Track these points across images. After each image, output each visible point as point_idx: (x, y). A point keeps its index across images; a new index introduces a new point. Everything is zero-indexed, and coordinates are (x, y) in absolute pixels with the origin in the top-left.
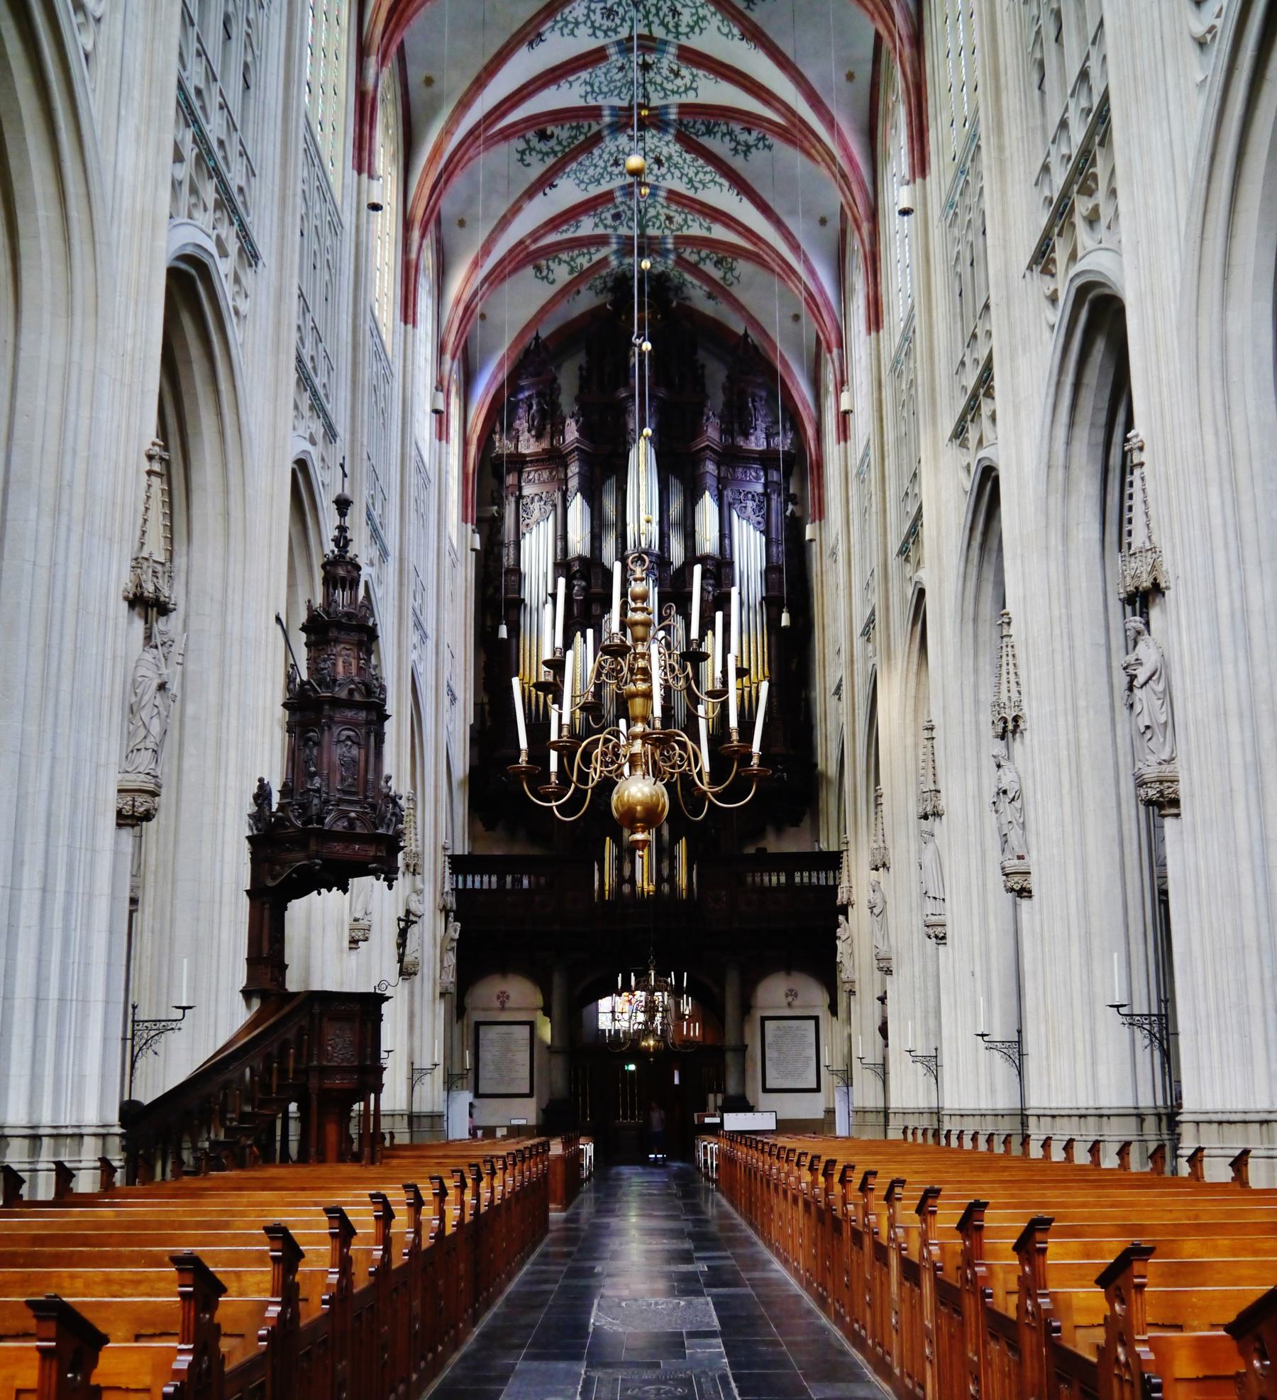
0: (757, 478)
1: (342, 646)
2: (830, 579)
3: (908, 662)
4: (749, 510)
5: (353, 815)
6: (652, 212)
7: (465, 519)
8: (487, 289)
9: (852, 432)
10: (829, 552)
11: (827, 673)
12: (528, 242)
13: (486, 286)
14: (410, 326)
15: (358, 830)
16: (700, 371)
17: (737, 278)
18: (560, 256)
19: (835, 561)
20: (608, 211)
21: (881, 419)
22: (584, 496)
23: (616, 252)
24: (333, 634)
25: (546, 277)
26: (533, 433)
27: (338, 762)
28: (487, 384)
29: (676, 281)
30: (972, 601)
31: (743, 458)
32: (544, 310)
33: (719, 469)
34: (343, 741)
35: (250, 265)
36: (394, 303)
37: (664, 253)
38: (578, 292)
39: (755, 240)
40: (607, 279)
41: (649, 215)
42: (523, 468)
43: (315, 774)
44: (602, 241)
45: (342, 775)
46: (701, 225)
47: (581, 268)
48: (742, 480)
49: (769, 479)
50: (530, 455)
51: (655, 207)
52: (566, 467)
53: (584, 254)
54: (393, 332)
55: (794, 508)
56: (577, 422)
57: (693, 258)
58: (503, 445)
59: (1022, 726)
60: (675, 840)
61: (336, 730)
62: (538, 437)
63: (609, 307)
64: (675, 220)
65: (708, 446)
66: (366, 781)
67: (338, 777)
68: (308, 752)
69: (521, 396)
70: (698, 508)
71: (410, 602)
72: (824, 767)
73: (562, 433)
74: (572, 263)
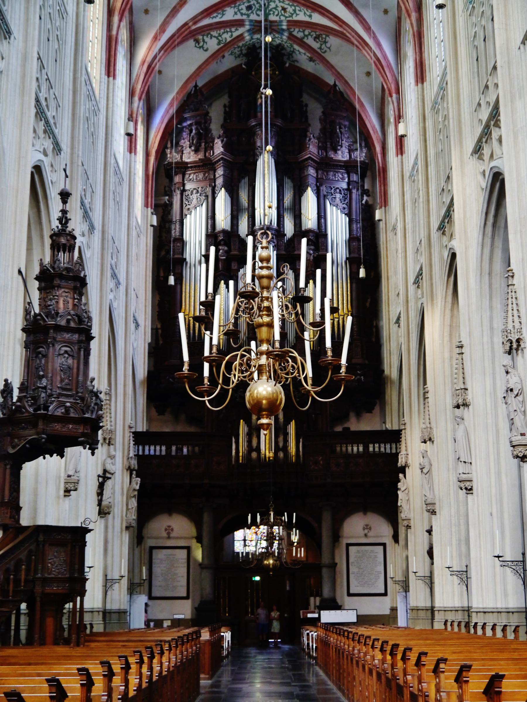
0: (343, 179)
1: (63, 290)
2: (392, 246)
3: (445, 302)
4: (338, 199)
5: (68, 404)
7: (146, 205)
8: (163, 54)
9: (406, 149)
10: (391, 228)
11: (390, 309)
12: (191, 24)
13: (162, 52)
14: (111, 78)
15: (72, 415)
16: (305, 108)
18: (212, 33)
19: (396, 234)
20: (243, 4)
21: (425, 141)
22: (227, 190)
23: (248, 31)
24: (57, 282)
25: (202, 47)
26: (193, 148)
27: (59, 368)
28: (162, 117)
29: (288, 49)
30: (488, 261)
31: (334, 165)
32: (200, 69)
33: (317, 172)
34: (62, 354)
35: (6, 38)
36: (101, 63)
37: (281, 32)
38: (223, 57)
39: (340, 23)
40: (243, 48)
41: (271, 7)
42: (186, 171)
43: (43, 376)
44: (239, 23)
45: (61, 377)
46: (305, 13)
47: (226, 41)
48: (332, 180)
49: (351, 179)
50: (190, 163)
52: (215, 171)
53: (227, 32)
54: (100, 82)
55: (368, 199)
56: (222, 141)
57: (300, 35)
58: (173, 156)
59: (522, 345)
60: (287, 422)
61: (57, 347)
62: (196, 151)
63: (244, 66)
64: (288, 10)
65: (310, 157)
66: (78, 381)
67: (59, 378)
68: (38, 361)
69: (185, 124)
70: (303, 199)
71: (108, 261)
72: (389, 373)
73: (212, 148)
74: (220, 38)
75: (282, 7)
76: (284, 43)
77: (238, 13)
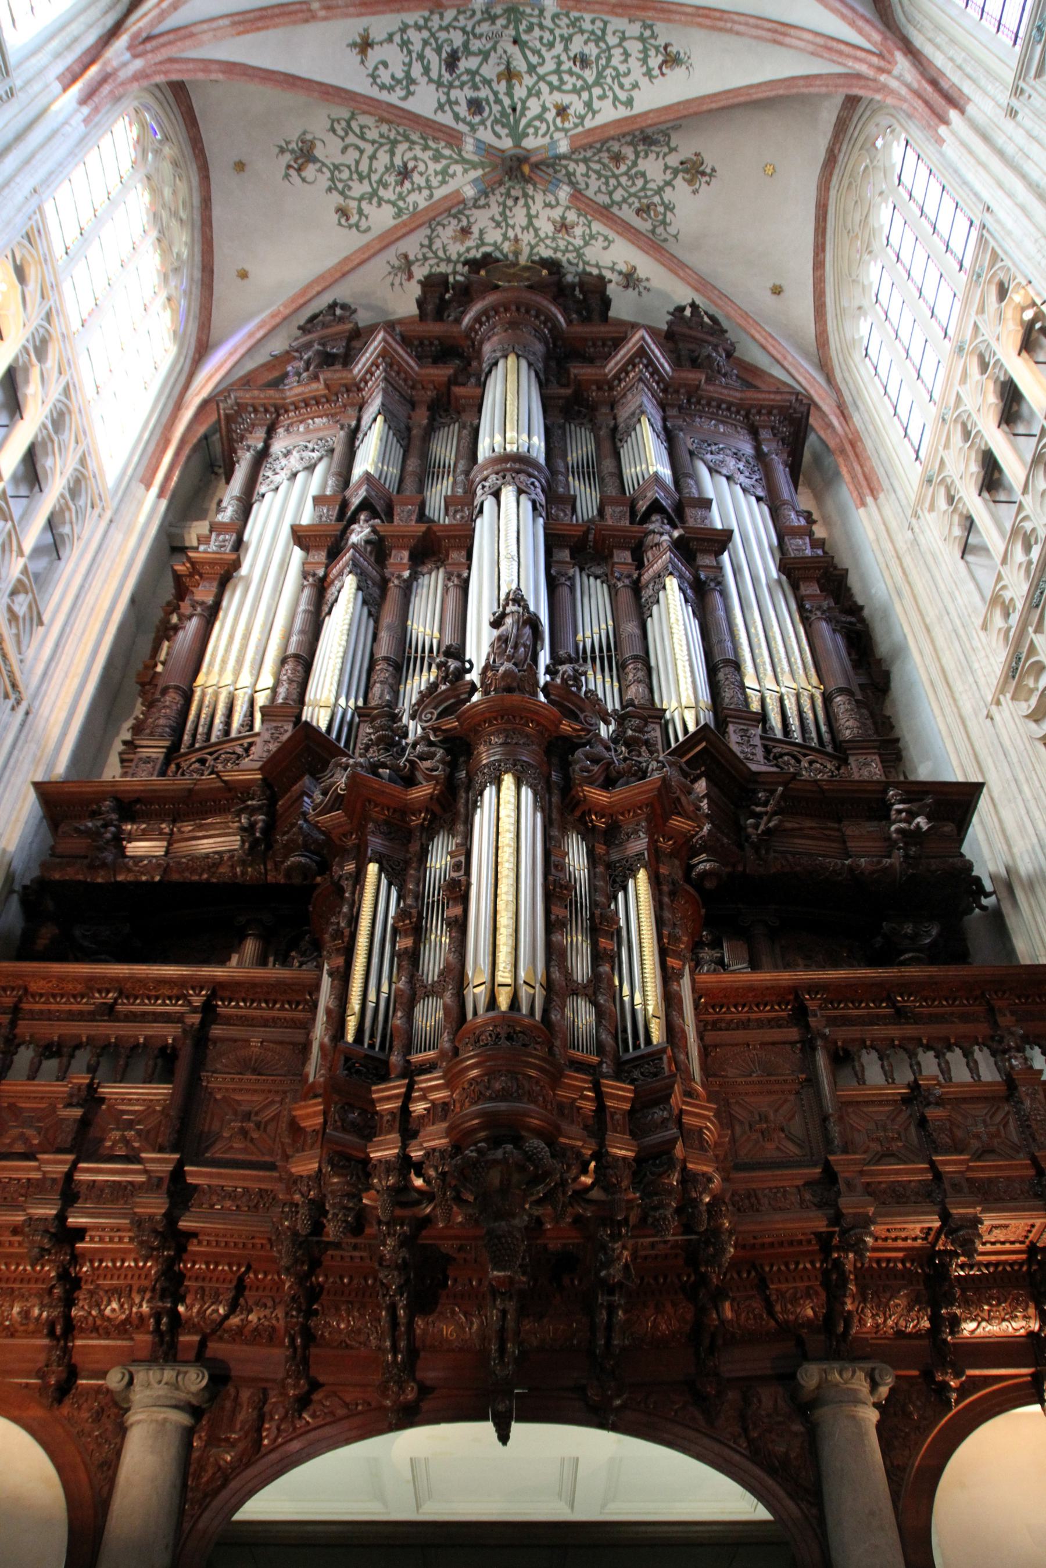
6: (534, 107)
17: (675, 236)
25: (357, 226)
41: (530, 114)
46: (616, 98)
51: (538, 94)
53: (420, 189)
64: (571, 111)
74: (401, 203)
75: (556, 106)
76: (559, 255)
77: (447, 108)
